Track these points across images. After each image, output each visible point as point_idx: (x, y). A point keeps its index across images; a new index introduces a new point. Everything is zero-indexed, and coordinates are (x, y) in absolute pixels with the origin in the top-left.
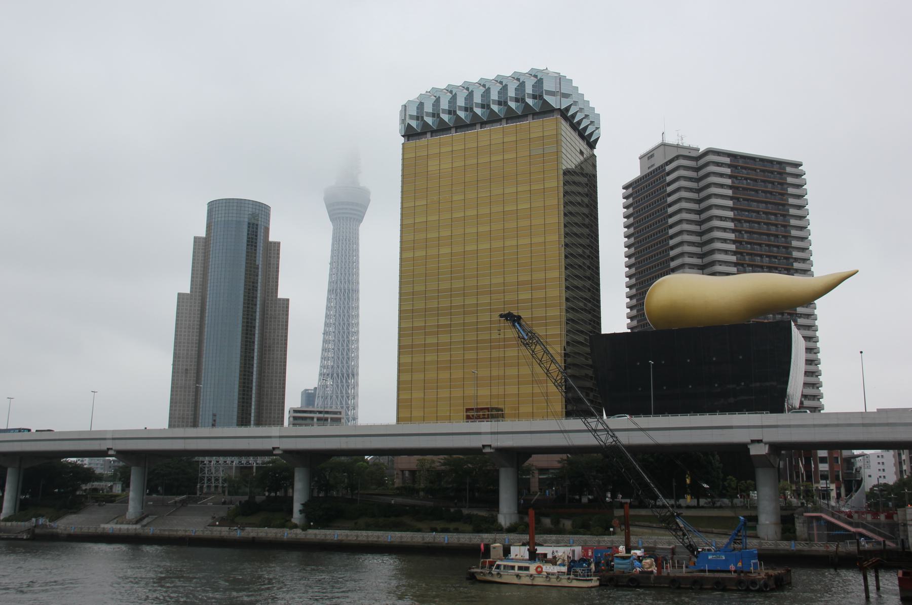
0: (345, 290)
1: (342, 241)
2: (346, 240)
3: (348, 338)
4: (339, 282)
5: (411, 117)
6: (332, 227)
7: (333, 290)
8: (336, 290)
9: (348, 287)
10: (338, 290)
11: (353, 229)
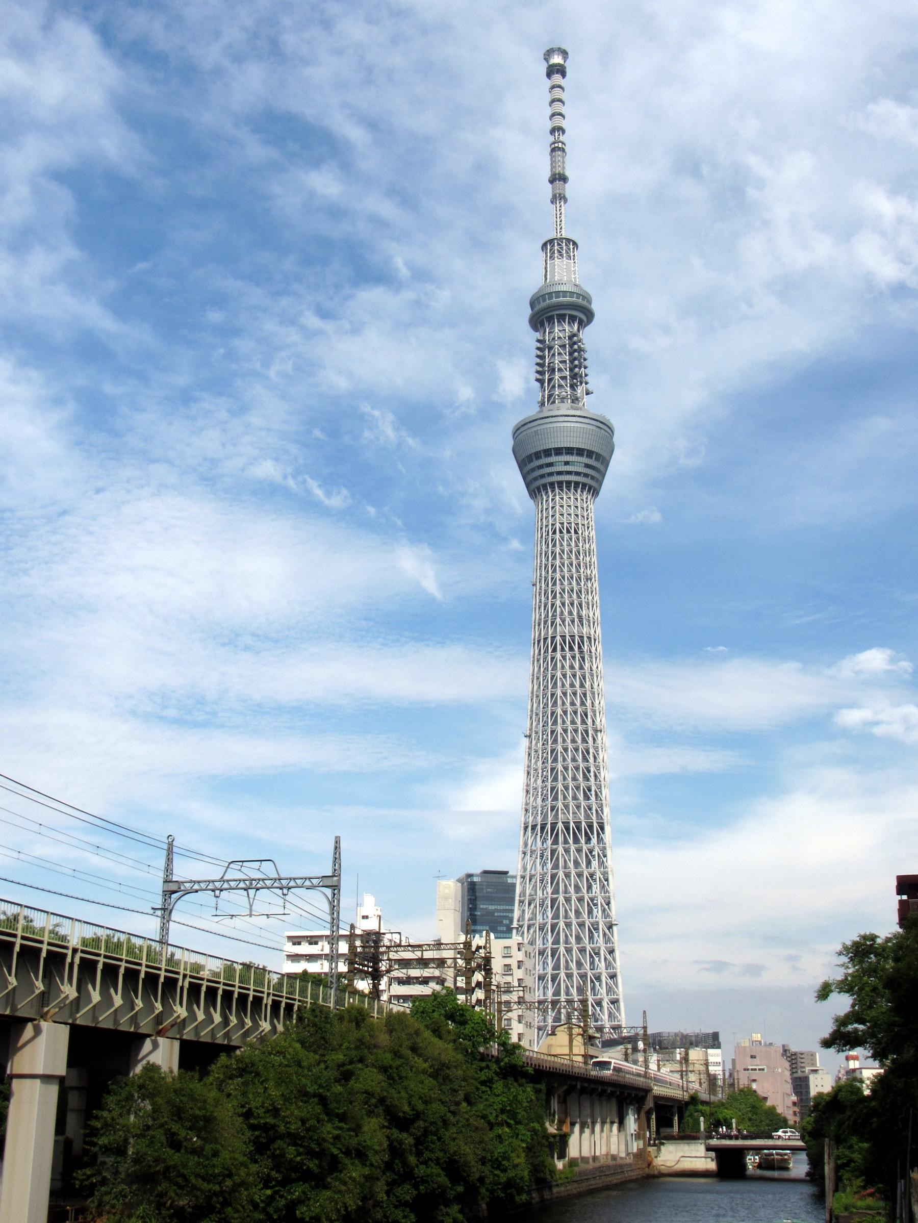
0: (572, 637)
1: (561, 532)
2: (568, 532)
4: (558, 620)
7: (545, 639)
8: (553, 638)
10: (558, 638)
11: (583, 508)
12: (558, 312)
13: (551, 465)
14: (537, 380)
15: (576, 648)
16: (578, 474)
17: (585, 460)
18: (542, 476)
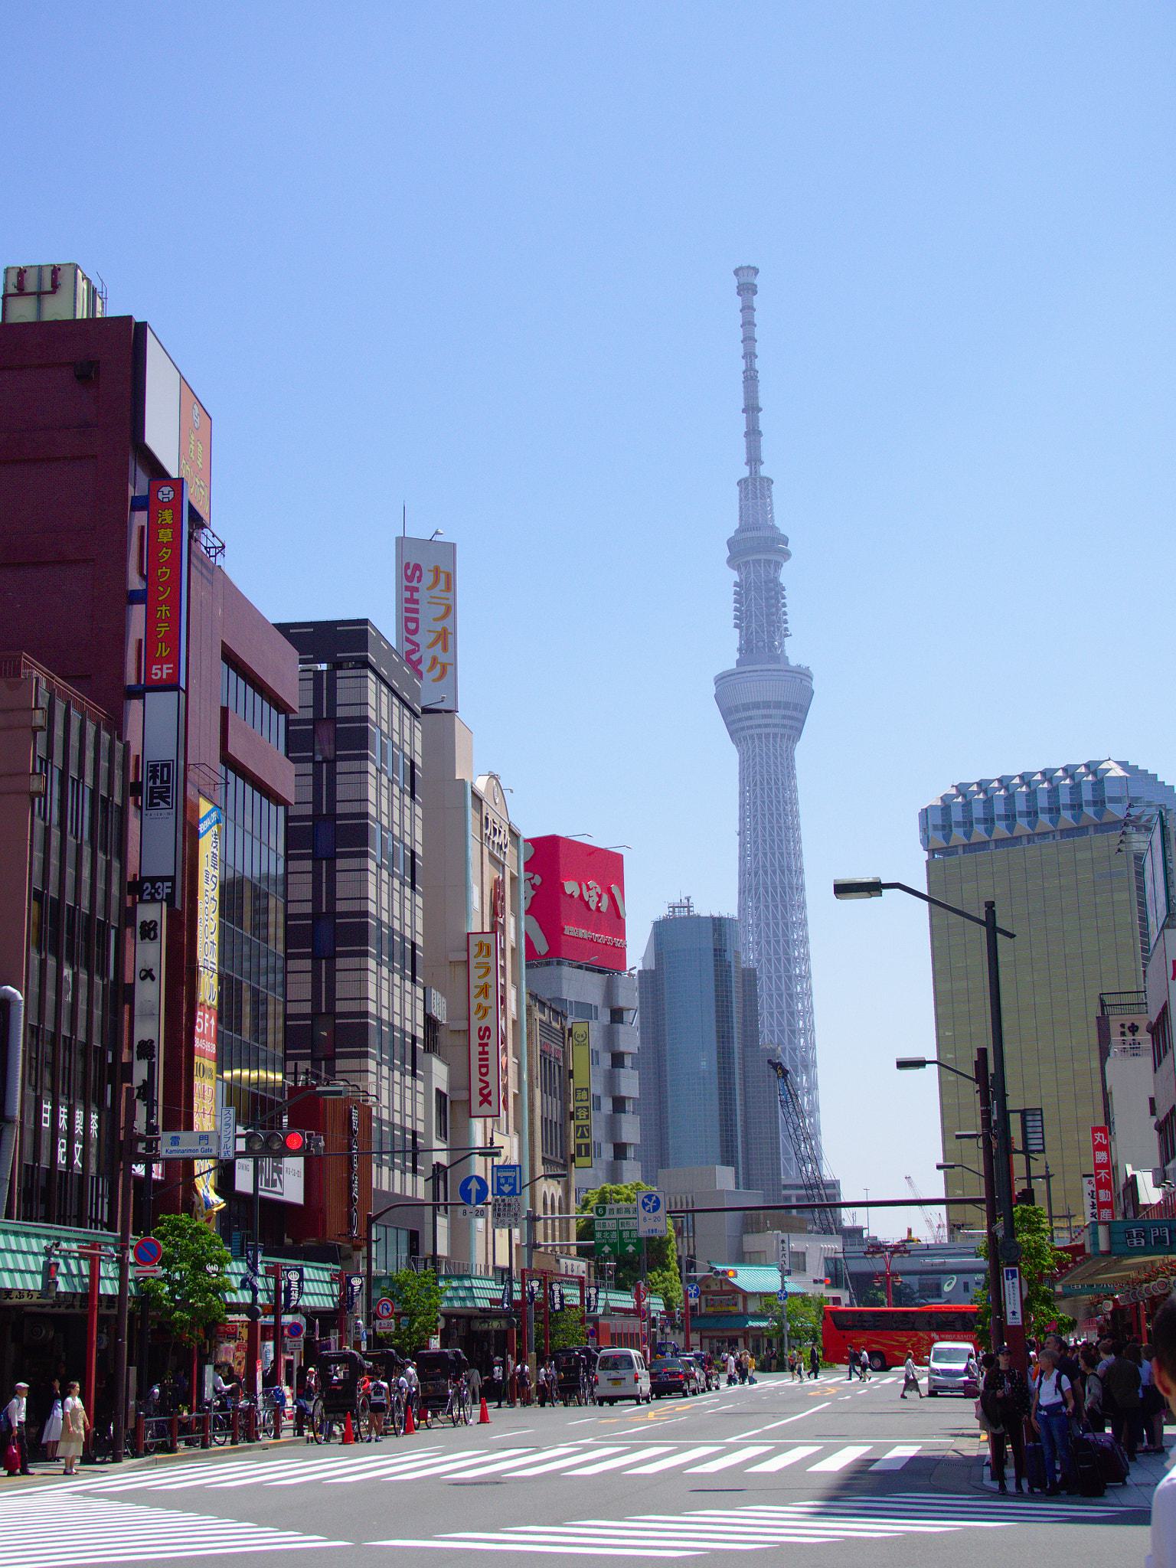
1: (762, 784)
2: (768, 783)
3: (789, 989)
4: (761, 872)
5: (935, 827)
6: (738, 756)
7: (750, 891)
8: (757, 889)
9: (781, 882)
12: (754, 557)
13: (751, 718)
14: (736, 626)
15: (778, 899)
16: (775, 726)
17: (783, 712)
18: (742, 729)
